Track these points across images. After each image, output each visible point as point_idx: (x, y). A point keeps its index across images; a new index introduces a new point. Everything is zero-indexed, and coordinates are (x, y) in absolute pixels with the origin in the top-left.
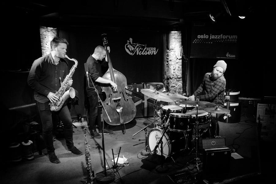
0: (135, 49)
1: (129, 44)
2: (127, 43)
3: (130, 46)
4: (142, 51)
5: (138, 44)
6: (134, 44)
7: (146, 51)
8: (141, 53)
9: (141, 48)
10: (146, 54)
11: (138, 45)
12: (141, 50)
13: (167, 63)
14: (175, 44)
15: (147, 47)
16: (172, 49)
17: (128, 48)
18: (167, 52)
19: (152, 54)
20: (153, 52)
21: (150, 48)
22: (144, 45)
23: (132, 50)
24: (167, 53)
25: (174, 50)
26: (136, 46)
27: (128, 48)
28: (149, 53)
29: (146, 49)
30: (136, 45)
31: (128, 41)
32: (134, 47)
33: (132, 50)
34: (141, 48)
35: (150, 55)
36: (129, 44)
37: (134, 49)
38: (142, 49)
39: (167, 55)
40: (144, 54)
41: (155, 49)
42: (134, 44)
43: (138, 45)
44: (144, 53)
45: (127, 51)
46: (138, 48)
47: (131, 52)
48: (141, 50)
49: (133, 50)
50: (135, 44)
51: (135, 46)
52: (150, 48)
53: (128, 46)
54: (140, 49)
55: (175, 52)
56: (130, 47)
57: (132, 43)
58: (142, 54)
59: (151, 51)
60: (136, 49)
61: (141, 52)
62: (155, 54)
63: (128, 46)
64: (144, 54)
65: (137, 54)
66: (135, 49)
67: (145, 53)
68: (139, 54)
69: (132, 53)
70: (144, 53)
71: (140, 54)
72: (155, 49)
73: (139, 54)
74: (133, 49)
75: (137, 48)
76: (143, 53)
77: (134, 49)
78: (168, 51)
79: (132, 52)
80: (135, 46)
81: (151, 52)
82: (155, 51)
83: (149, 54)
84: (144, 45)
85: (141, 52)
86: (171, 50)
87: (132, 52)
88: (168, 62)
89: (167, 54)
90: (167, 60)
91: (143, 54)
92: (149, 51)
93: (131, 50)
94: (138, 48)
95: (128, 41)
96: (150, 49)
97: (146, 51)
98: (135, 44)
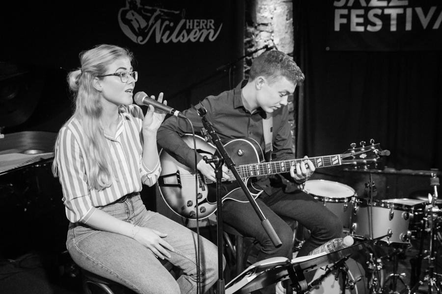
0: (150, 23)
1: (131, 9)
2: (125, 6)
3: (135, 13)
4: (172, 30)
5: (158, 10)
6: (146, 7)
7: (184, 32)
8: (167, 38)
9: (167, 23)
10: (184, 41)
11: (156, 14)
12: (167, 28)
13: (249, 68)
14: (272, 7)
15: (186, 18)
16: (266, 25)
17: (128, 22)
18: (249, 35)
19: (202, 40)
20: (205, 32)
21: (195, 21)
22: (178, 12)
23: (139, 28)
24: (247, 37)
25: (268, 28)
26: (152, 14)
27: (128, 22)
28: (192, 37)
29: (185, 23)
30: (154, 11)
32: (147, 19)
34: (167, 23)
35: (196, 42)
36: (131, 9)
37: (146, 24)
38: (172, 24)
39: (249, 42)
40: (179, 41)
41: (211, 23)
42: (146, 7)
43: (156, 14)
44: (177, 37)
46: (159, 21)
47: (137, 35)
48: (167, 28)
50: (150, 8)
51: (149, 15)
52: (195, 21)
53: (129, 16)
54: (163, 26)
55: (272, 32)
57: (139, 6)
58: (171, 40)
59: (200, 30)
60: (153, 25)
61: (168, 33)
62: (211, 39)
63: (129, 16)
64: (179, 41)
65: (158, 41)
66: (150, 23)
67: (180, 38)
68: (161, 40)
69: (140, 38)
70: (177, 37)
71: (165, 41)
72: (211, 23)
73: (161, 40)
74: (143, 24)
75: (156, 20)
76: (173, 38)
77: (146, 24)
78: (251, 30)
79: (142, 33)
80: (149, 15)
81: (198, 34)
82: (212, 32)
83: (193, 40)
84: (178, 12)
85: (168, 33)
86: (261, 27)
87: (142, 33)
88: (249, 63)
89: (248, 39)
90: (248, 58)
91: (175, 41)
92: (194, 31)
93: (136, 26)
94: (159, 21)
96: (196, 24)
97: (184, 32)
98: (150, 8)
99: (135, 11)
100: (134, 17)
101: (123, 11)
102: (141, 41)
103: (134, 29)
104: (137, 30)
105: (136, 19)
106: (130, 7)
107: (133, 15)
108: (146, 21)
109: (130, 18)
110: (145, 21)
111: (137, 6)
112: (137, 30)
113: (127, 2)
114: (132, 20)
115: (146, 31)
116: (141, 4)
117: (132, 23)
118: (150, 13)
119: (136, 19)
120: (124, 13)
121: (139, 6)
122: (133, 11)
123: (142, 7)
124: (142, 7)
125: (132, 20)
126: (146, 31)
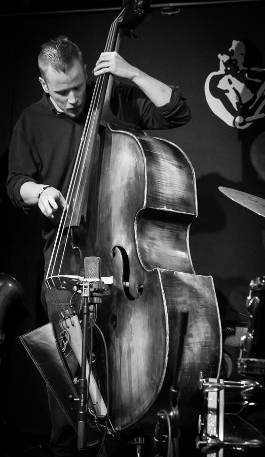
0: (259, 95)
1: (227, 73)
2: (217, 69)
3: (233, 80)
6: (252, 69)
27: (220, 95)
31: (224, 58)
33: (244, 102)
36: (227, 73)
37: (252, 95)
42: (252, 69)
45: (216, 106)
49: (250, 102)
51: (257, 80)
53: (223, 84)
56: (229, 87)
57: (241, 68)
63: (223, 84)
66: (259, 95)
77: (252, 95)
80: (257, 80)
95: (224, 58)
99: (233, 76)
100: (232, 86)
101: (214, 77)
102: (240, 125)
103: (231, 105)
104: (235, 106)
105: (234, 88)
106: (226, 70)
107: (230, 82)
108: (252, 92)
109: (224, 88)
110: (250, 92)
111: (238, 69)
112: (235, 106)
113: (221, 64)
114: (227, 91)
115: (250, 108)
116: (244, 65)
117: (226, 94)
118: (259, 79)
119: (234, 88)
120: (215, 80)
121: (241, 68)
122: (230, 76)
123: (246, 69)
124: (246, 69)
125: (227, 91)
126: (250, 108)
